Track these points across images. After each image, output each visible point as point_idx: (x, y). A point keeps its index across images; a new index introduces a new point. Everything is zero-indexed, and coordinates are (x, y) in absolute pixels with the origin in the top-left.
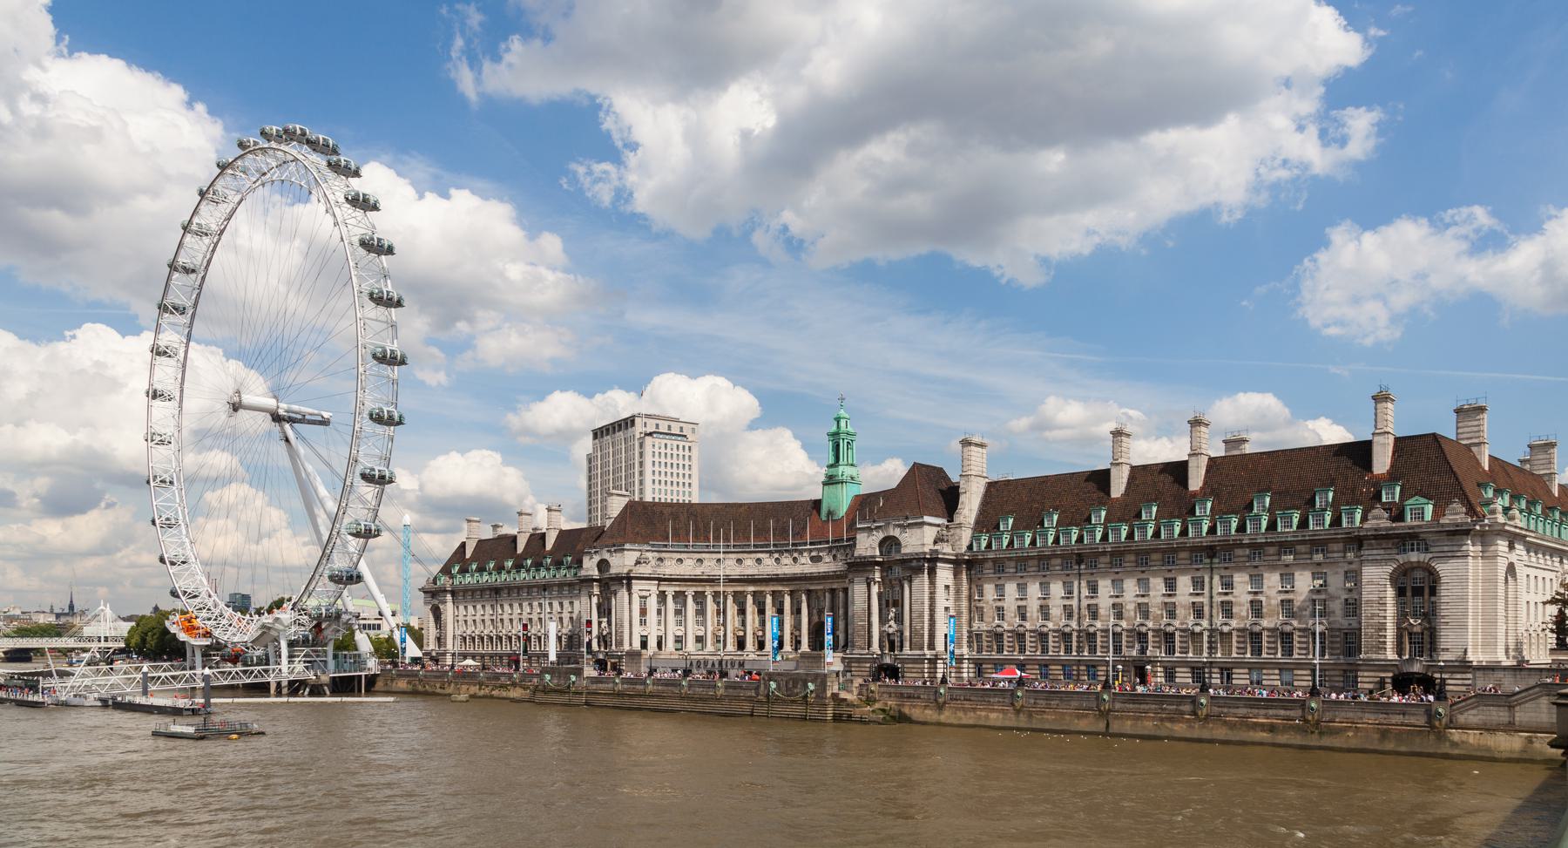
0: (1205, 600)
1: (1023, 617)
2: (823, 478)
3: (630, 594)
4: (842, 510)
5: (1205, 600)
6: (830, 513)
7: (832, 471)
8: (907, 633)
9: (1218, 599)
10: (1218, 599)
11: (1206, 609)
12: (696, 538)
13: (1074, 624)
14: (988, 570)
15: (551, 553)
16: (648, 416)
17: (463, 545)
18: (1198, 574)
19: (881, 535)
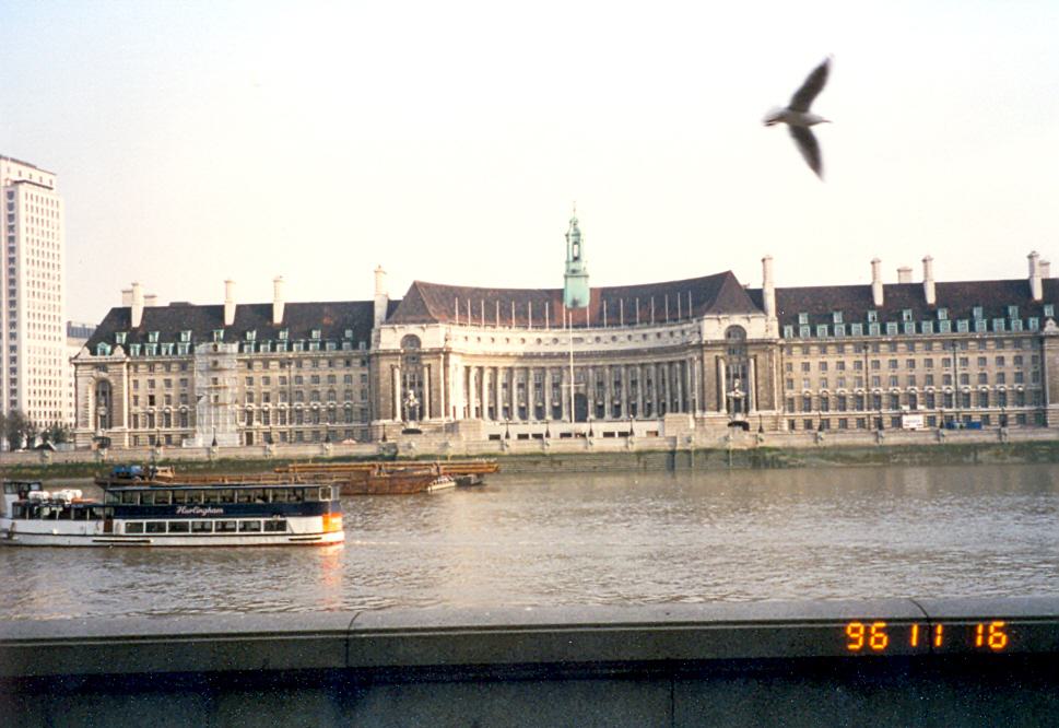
0: (952, 373)
1: (825, 385)
2: (564, 272)
3: (446, 366)
4: (586, 302)
5: (952, 373)
6: (575, 303)
7: (573, 266)
8: (752, 398)
9: (959, 372)
10: (959, 372)
11: (953, 379)
12: (474, 318)
13: (863, 389)
14: (796, 351)
15: (283, 326)
16: (13, 160)
17: (120, 316)
18: (947, 356)
19: (726, 324)
